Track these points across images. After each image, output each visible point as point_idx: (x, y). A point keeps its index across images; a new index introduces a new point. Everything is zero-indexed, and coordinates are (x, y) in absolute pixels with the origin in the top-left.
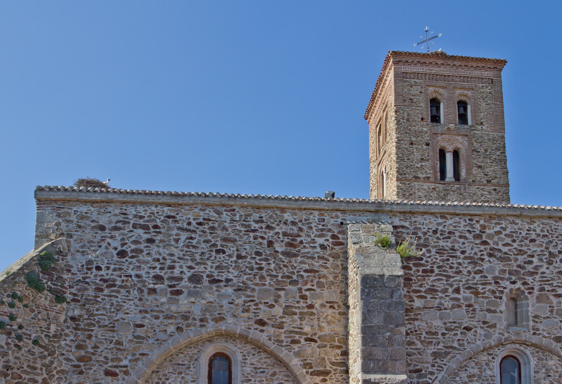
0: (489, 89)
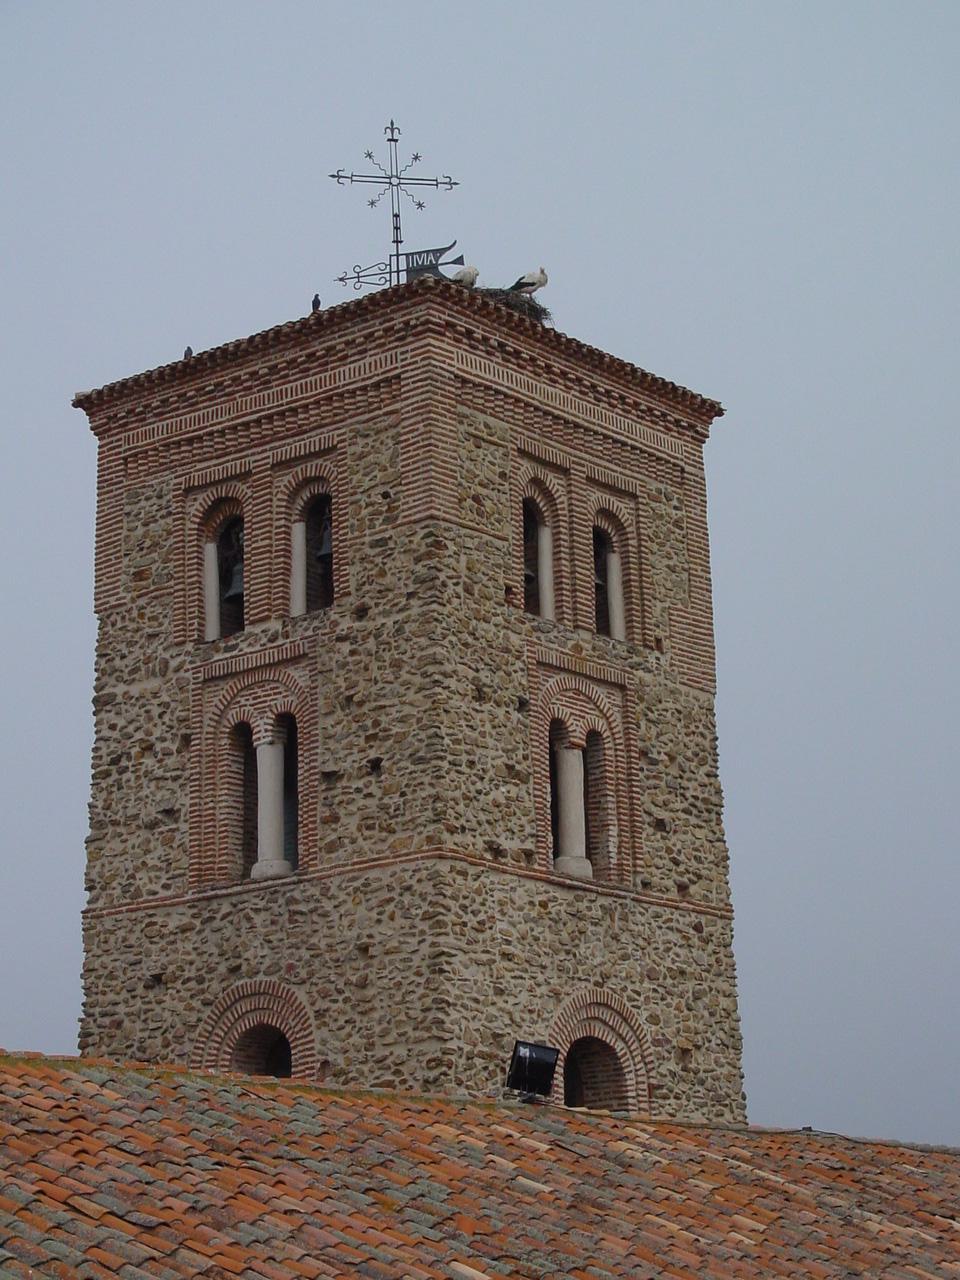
0: (676, 508)
